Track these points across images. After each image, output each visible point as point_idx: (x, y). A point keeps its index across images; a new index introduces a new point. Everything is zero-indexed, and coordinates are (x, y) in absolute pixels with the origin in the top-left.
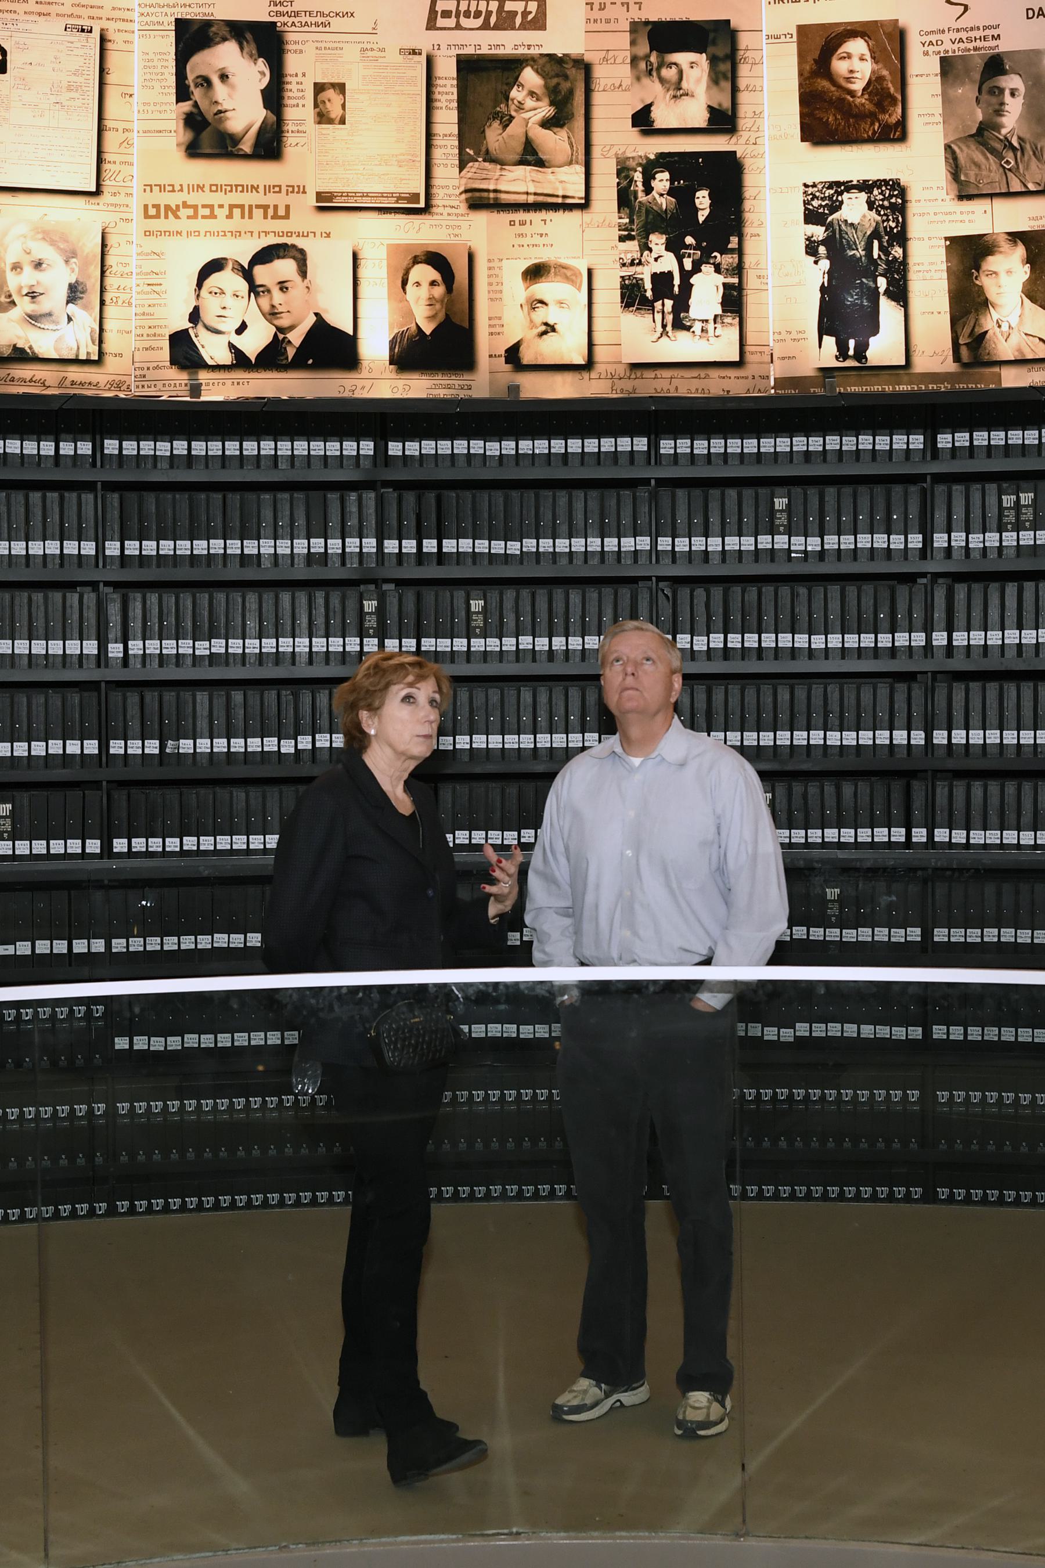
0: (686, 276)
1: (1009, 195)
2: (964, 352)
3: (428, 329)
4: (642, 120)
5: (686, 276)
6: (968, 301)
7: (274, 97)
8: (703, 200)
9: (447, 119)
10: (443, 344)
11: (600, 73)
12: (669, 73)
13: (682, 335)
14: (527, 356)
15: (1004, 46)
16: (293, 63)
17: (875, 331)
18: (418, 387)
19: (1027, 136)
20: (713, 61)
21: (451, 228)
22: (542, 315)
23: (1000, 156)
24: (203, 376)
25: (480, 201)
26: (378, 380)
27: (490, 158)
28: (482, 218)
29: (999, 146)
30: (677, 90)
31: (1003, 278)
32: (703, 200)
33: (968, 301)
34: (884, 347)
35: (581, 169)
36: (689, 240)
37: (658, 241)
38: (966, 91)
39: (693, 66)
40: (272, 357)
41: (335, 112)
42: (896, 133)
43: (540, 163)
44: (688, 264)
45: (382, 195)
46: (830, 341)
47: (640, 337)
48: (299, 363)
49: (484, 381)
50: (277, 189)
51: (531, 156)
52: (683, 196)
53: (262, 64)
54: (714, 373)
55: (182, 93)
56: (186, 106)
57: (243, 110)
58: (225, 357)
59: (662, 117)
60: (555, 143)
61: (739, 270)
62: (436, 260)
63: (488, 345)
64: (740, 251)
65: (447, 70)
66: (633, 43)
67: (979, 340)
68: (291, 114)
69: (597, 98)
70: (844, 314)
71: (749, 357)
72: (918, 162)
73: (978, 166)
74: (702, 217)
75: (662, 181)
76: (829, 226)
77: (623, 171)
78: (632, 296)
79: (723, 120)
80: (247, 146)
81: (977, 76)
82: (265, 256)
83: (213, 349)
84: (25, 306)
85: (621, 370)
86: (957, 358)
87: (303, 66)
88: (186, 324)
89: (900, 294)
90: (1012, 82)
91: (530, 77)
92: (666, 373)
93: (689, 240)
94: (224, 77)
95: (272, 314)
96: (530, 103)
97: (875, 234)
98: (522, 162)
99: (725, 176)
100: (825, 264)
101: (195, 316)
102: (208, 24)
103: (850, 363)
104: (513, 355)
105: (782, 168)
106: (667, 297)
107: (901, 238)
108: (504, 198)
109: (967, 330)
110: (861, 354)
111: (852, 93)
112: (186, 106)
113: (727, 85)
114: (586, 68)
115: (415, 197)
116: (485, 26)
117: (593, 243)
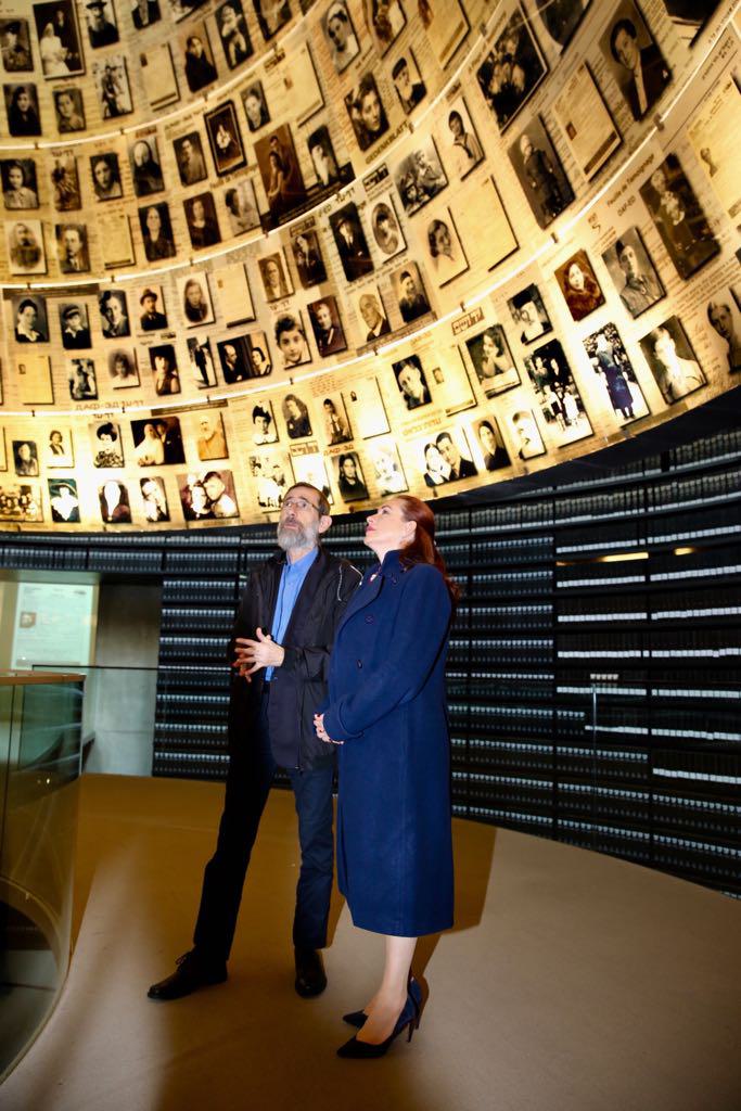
0: (561, 400)
1: (650, 307)
2: (667, 396)
3: (493, 452)
4: (524, 339)
5: (561, 400)
6: (659, 370)
7: (423, 380)
8: (554, 364)
9: (471, 366)
10: (499, 459)
11: (505, 327)
12: (524, 316)
13: (570, 427)
14: (526, 455)
15: (619, 235)
16: (425, 366)
17: (632, 400)
18: (499, 477)
19: (644, 274)
20: (535, 303)
21: (488, 409)
22: (524, 435)
23: (638, 289)
24: (437, 489)
25: (491, 395)
26: (486, 478)
27: (488, 377)
28: (494, 400)
29: (636, 285)
30: (528, 320)
31: (665, 350)
32: (554, 364)
33: (659, 370)
34: (639, 410)
35: (513, 369)
36: (557, 384)
37: (547, 388)
38: (615, 265)
39: (529, 307)
40: (453, 478)
41: (440, 379)
42: (601, 301)
43: (502, 372)
44: (561, 396)
45: (462, 405)
46: (619, 411)
47: (557, 434)
48: (461, 477)
49: (515, 471)
50: (434, 413)
51: (499, 371)
52: (547, 365)
53: (417, 370)
54: (587, 442)
55: (401, 389)
56: (403, 393)
57: (417, 390)
58: (441, 481)
59: (530, 337)
60: (503, 362)
61: (577, 391)
62: (486, 424)
63: (513, 454)
64: (574, 382)
65: (464, 348)
66: (510, 309)
67: (670, 388)
68: (429, 384)
69: (508, 337)
70: (620, 399)
71: (596, 431)
72: (613, 311)
73: (633, 299)
74: (557, 372)
75: (539, 361)
76: (598, 356)
77: (527, 364)
78: (549, 417)
79: (548, 327)
80: (422, 401)
81: (616, 256)
82: (439, 439)
83: (437, 480)
84: (384, 476)
85: (556, 450)
86: (667, 402)
87: (427, 366)
88: (427, 471)
89: (633, 378)
90: (628, 250)
91: (487, 339)
92: (571, 448)
93: (557, 384)
94: (409, 379)
95: (448, 460)
96: (491, 349)
97: (614, 353)
98: (497, 374)
99: (553, 351)
100: (603, 375)
101: (428, 468)
102: (399, 363)
103: (630, 420)
104: (521, 455)
105: (573, 336)
106: (555, 413)
107: (622, 350)
108: (497, 391)
109: (664, 386)
110: (632, 415)
111: (580, 291)
112: (403, 393)
113: (542, 310)
114: (500, 327)
115: (472, 402)
116: (469, 326)
117: (530, 399)
